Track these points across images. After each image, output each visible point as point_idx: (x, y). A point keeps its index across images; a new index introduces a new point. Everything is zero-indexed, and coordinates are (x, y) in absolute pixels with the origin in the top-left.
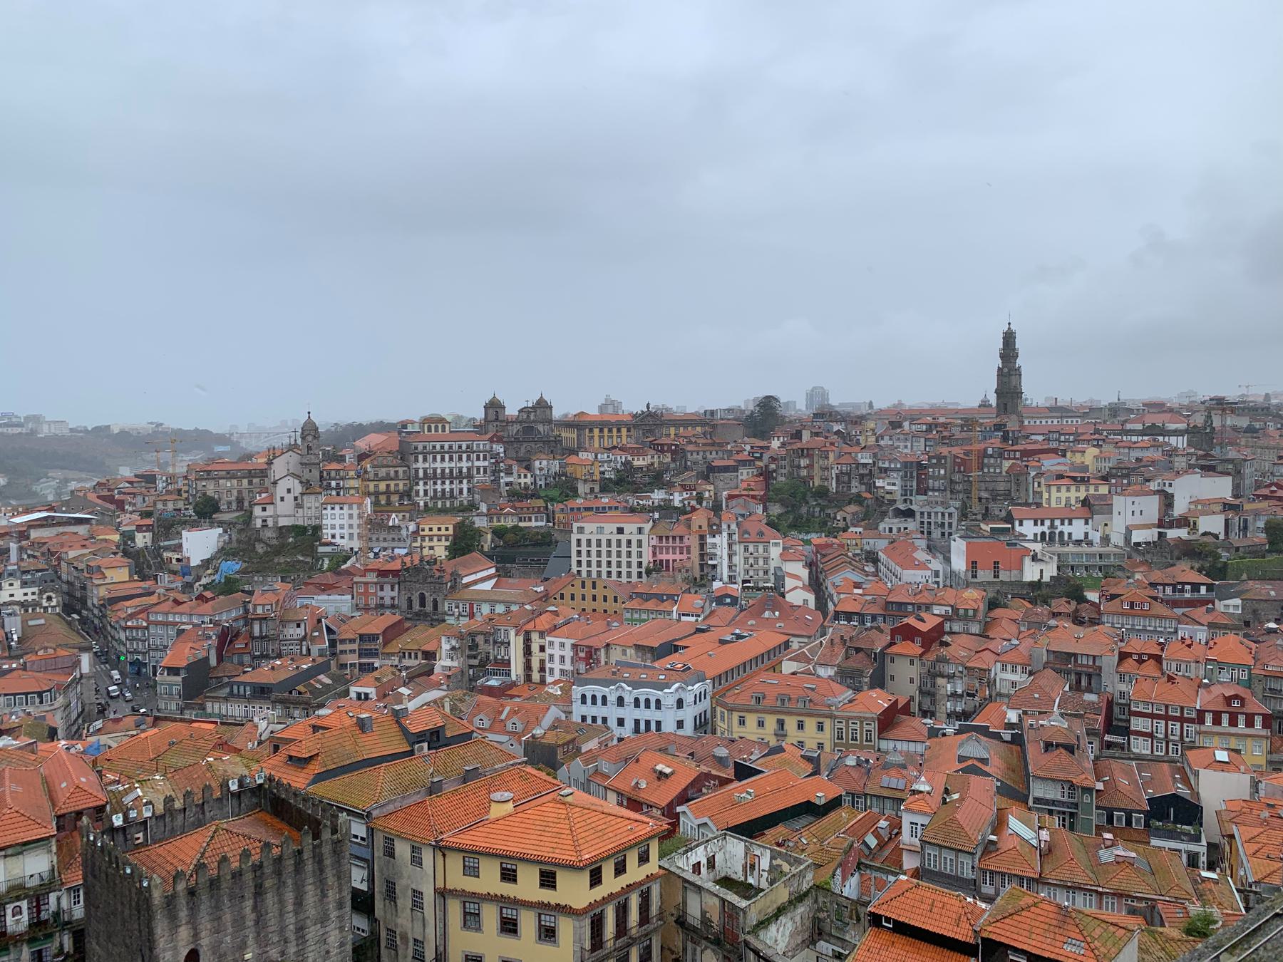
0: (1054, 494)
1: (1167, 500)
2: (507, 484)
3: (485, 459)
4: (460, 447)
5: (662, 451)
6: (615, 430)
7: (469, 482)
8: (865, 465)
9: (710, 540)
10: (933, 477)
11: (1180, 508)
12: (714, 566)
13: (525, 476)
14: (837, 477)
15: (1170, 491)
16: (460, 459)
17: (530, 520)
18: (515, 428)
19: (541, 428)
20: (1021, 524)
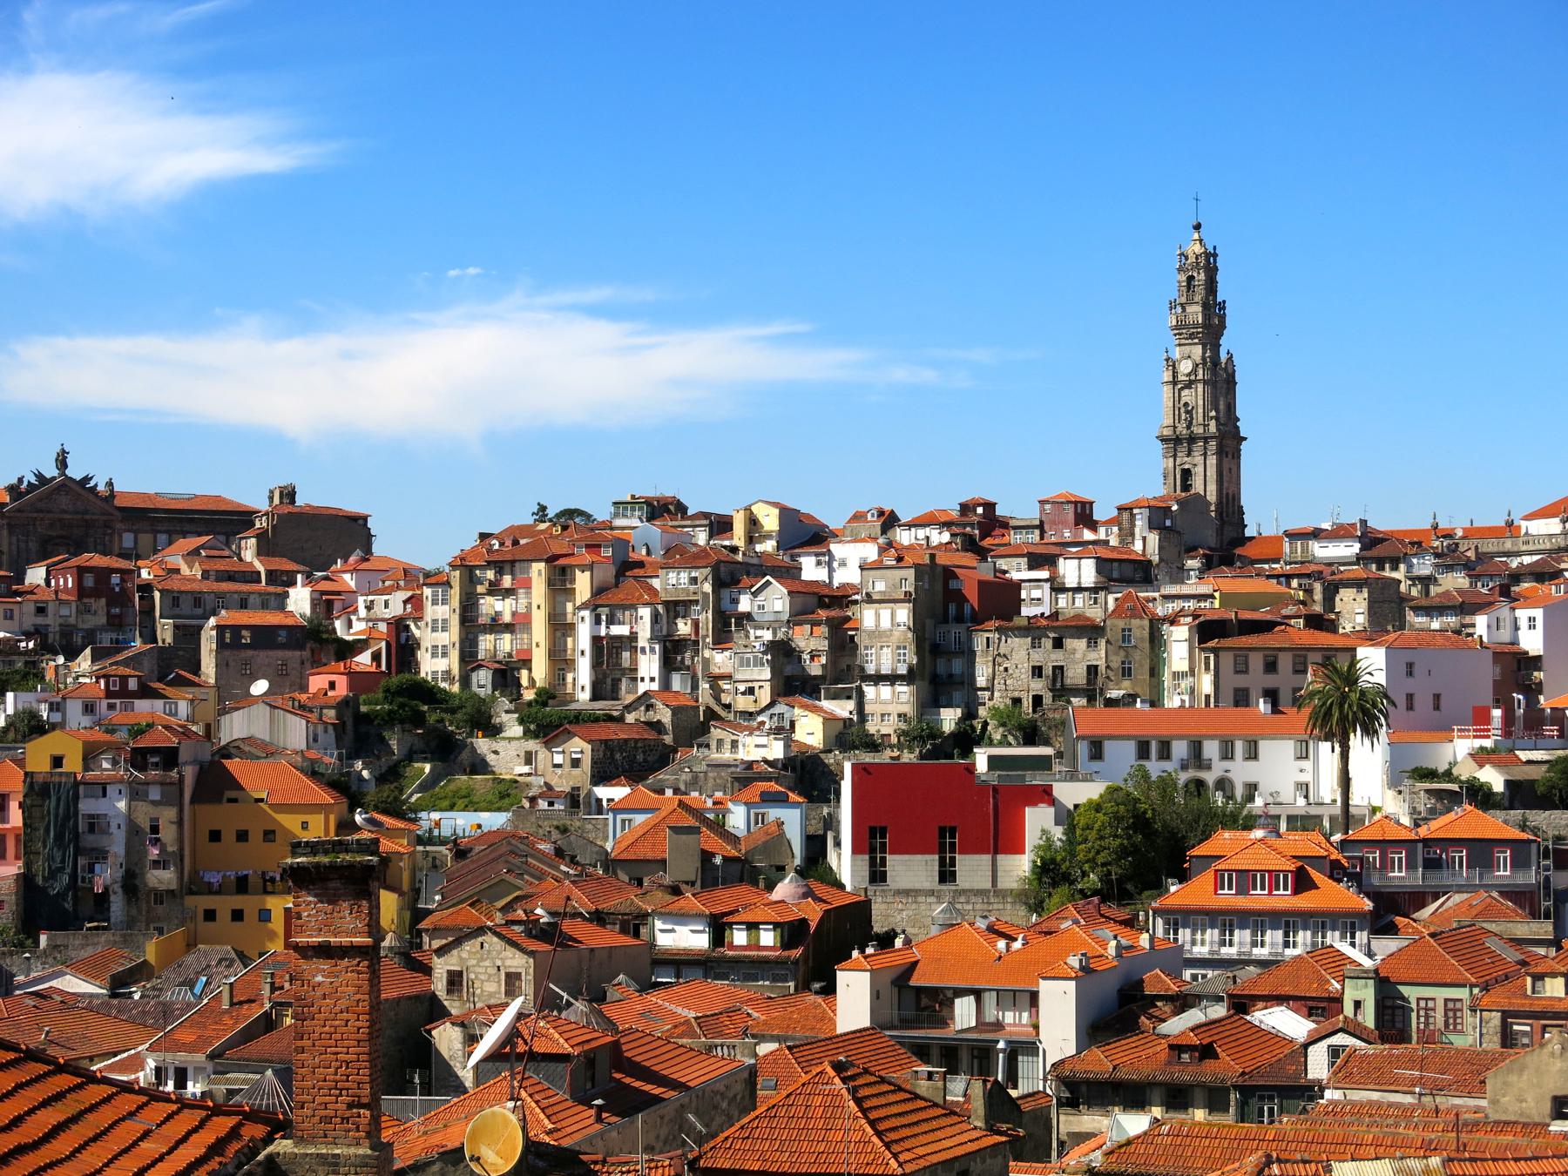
8: (677, 608)
10: (877, 634)
14: (596, 640)
15: (1532, 642)
20: (1097, 752)
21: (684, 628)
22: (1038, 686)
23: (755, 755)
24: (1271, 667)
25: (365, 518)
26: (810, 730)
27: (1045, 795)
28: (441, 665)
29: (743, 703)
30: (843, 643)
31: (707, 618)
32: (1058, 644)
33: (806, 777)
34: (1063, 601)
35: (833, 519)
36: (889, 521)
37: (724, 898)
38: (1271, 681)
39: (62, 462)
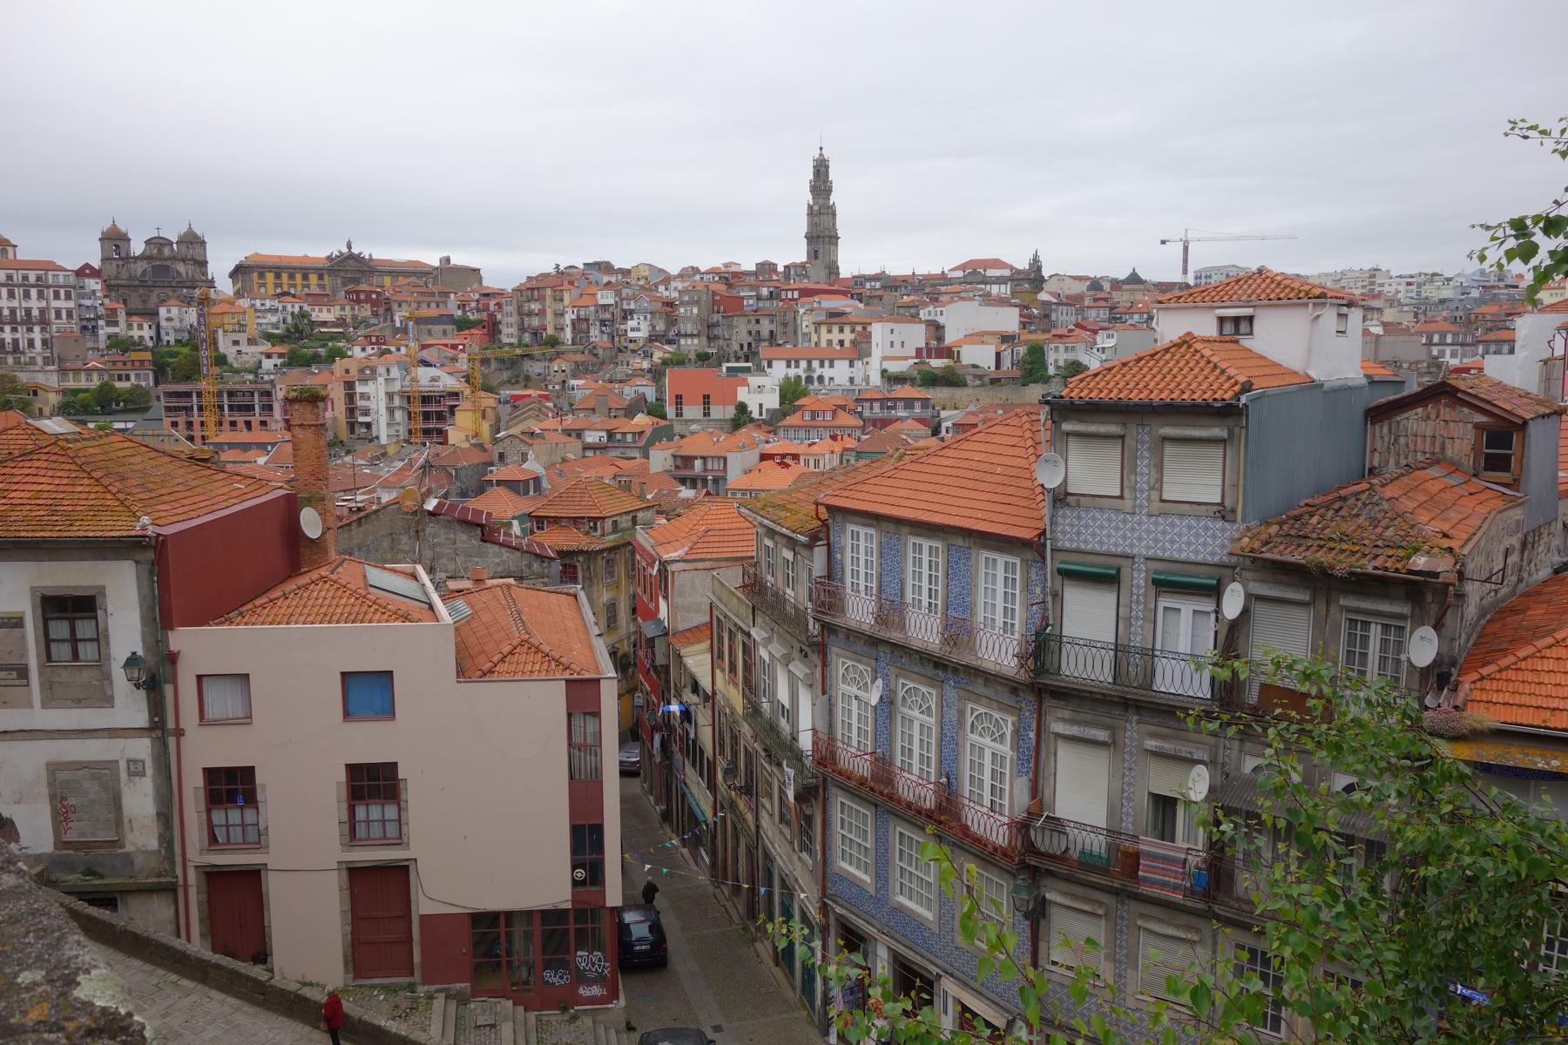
0: (825, 336)
1: (937, 329)
2: (109, 337)
3: (68, 297)
4: (25, 278)
5: (358, 301)
6: (299, 277)
7: (43, 330)
8: (605, 307)
9: (359, 389)
10: (686, 318)
11: (950, 338)
12: (368, 425)
13: (140, 327)
14: (573, 322)
15: (941, 320)
16: (27, 295)
17: (128, 378)
18: (139, 268)
19: (181, 268)
20: (770, 366)
21: (607, 316)
22: (750, 339)
23: (637, 366)
24: (841, 331)
25: (476, 271)
26: (658, 356)
27: (745, 383)
28: (511, 330)
29: (632, 346)
30: (672, 321)
31: (617, 312)
32: (758, 321)
33: (656, 374)
34: (761, 304)
35: (674, 270)
36: (695, 270)
37: (613, 424)
38: (841, 337)
39: (349, 247)
